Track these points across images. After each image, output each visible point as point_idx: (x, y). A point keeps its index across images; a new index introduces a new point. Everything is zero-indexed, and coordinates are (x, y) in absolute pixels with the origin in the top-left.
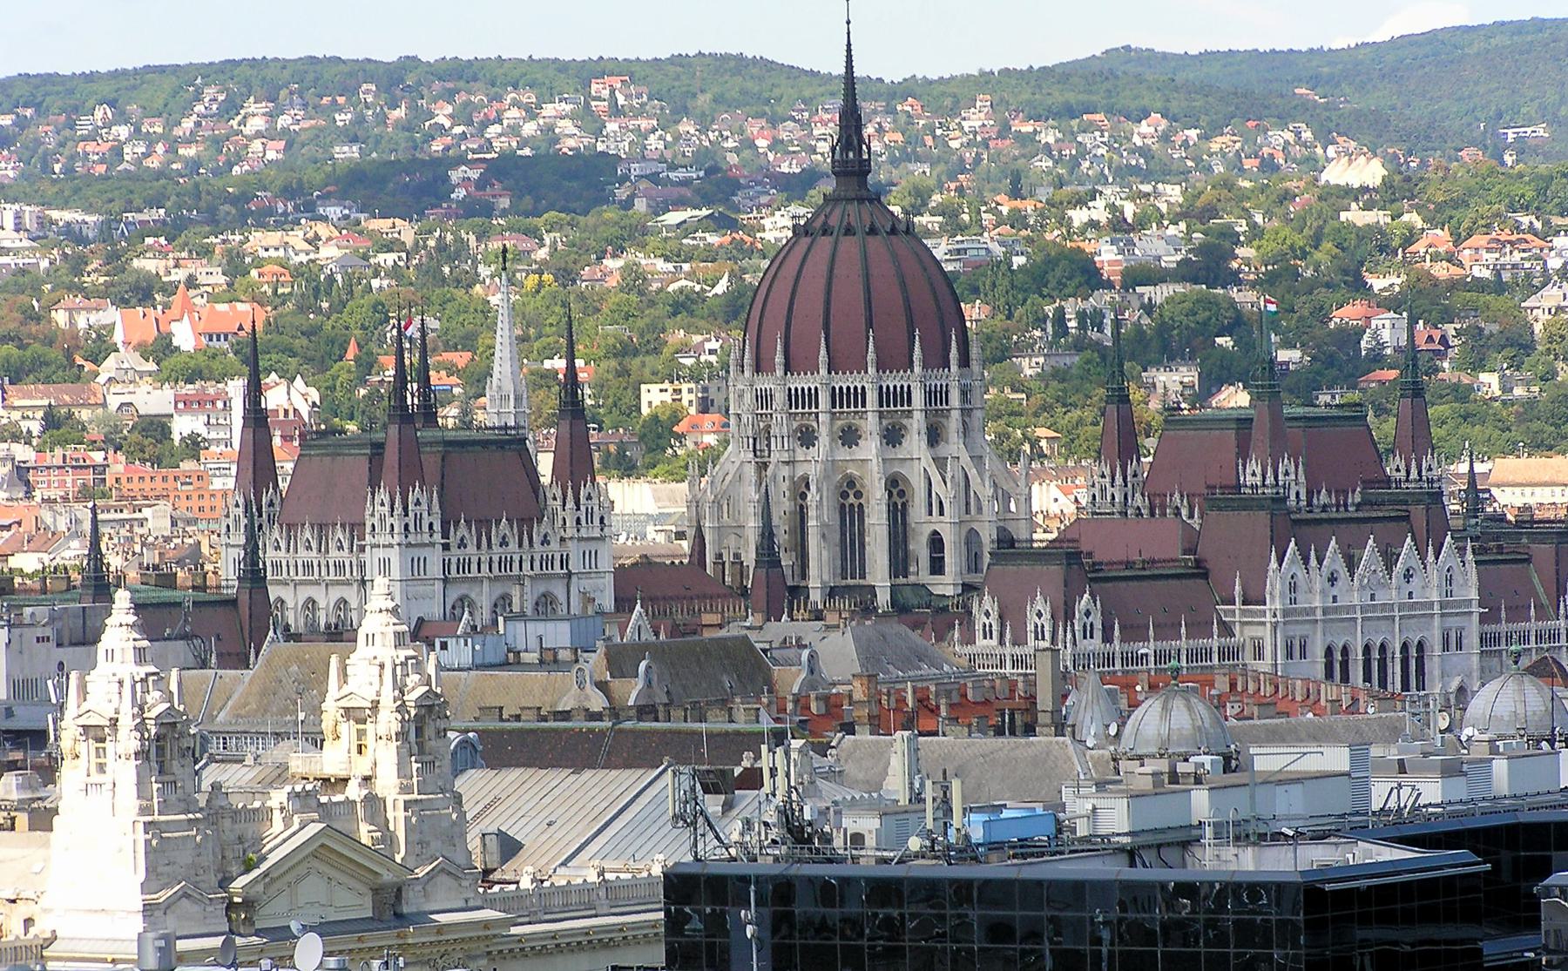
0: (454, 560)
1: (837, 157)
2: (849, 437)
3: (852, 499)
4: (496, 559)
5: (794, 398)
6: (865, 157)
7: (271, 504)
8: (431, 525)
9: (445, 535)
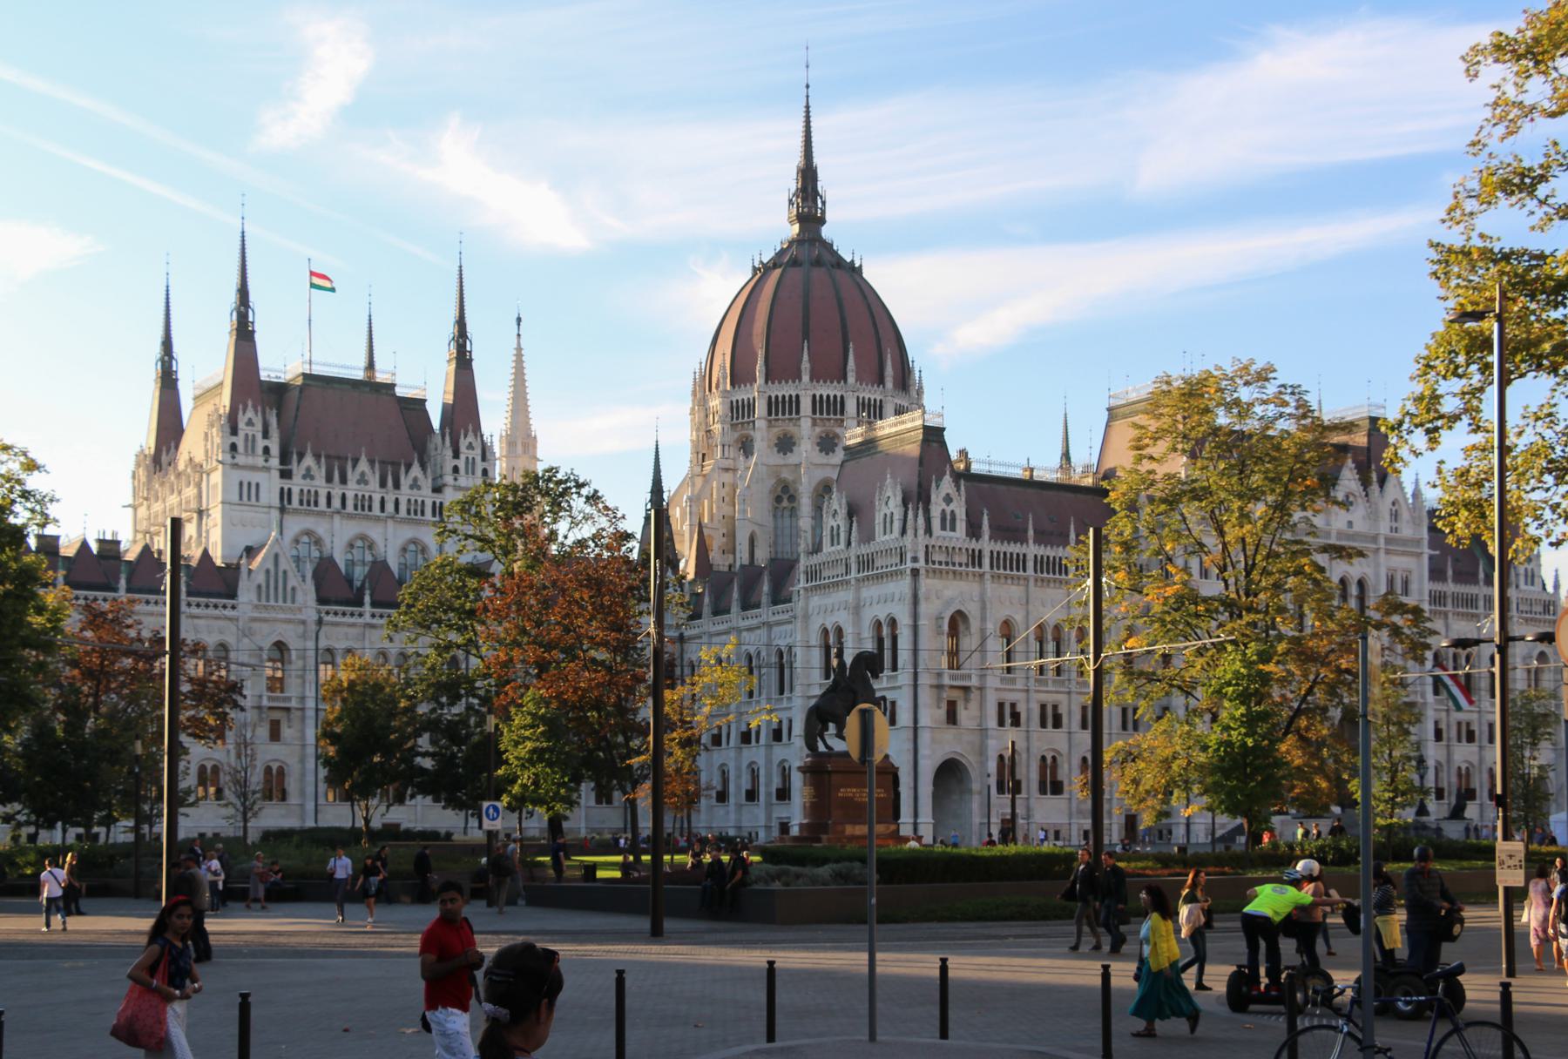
4: (350, 495)
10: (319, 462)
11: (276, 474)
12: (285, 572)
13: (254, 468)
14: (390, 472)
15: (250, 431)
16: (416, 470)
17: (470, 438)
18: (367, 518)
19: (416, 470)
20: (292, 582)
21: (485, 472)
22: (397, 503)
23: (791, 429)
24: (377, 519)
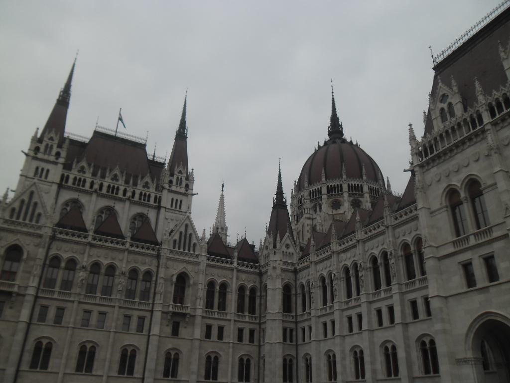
0: (72, 177)
4: (106, 184)
10: (89, 165)
11: (60, 167)
12: (36, 204)
14: (132, 177)
15: (50, 143)
16: (148, 179)
17: (181, 169)
20: (38, 211)
21: (187, 186)
22: (134, 193)
24: (120, 200)
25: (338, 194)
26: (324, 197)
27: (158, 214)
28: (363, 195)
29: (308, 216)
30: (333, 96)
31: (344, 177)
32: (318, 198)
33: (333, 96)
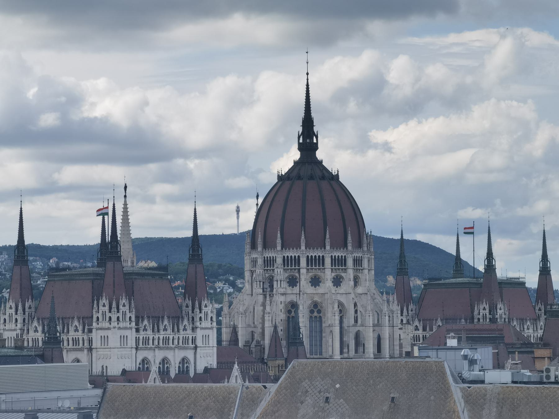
0: (141, 338)
1: (301, 141)
2: (315, 281)
3: (315, 314)
5: (286, 261)
6: (315, 141)
7: (30, 308)
8: (130, 318)
9: (137, 324)
11: (134, 330)
13: (126, 328)
18: (168, 348)
19: (186, 322)
23: (319, 273)
25: (319, 269)
26: (303, 271)
27: (195, 354)
28: (345, 269)
29: (282, 291)
30: (308, 79)
31: (328, 247)
32: (295, 269)
33: (308, 79)
